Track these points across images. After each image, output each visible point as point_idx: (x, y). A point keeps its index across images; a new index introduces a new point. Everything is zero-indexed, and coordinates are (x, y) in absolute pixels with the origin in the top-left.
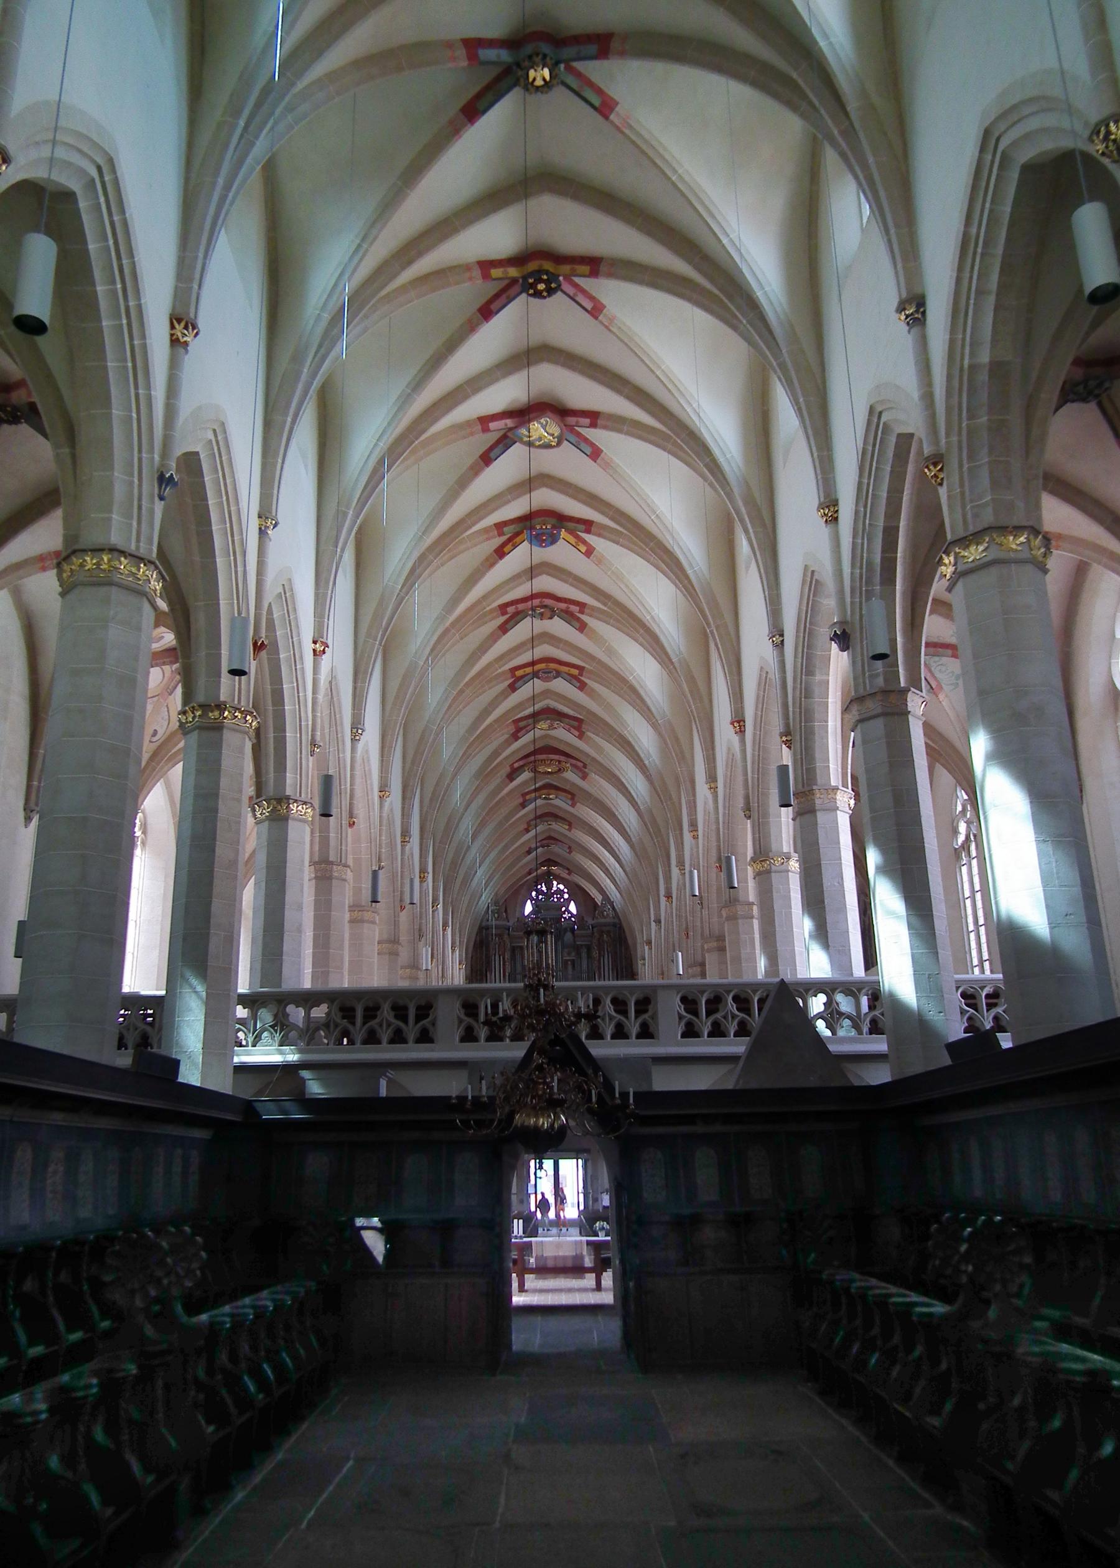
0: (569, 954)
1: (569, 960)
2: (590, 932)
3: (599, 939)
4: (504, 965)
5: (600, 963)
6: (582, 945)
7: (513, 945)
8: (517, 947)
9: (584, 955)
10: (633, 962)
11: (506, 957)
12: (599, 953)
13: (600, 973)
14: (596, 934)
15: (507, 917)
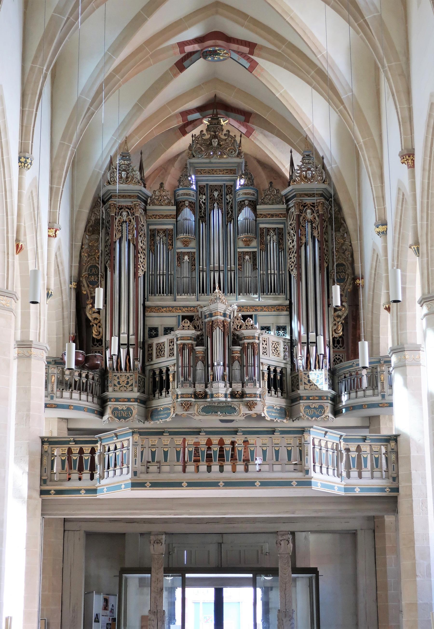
0: (247, 243)
1: (247, 253)
2: (285, 206)
3: (299, 216)
4: (136, 258)
5: (299, 257)
6: (268, 230)
7: (152, 227)
8: (159, 231)
9: (273, 246)
10: (357, 256)
11: (140, 244)
12: (299, 239)
13: (299, 275)
14: (293, 210)
15: (141, 179)
